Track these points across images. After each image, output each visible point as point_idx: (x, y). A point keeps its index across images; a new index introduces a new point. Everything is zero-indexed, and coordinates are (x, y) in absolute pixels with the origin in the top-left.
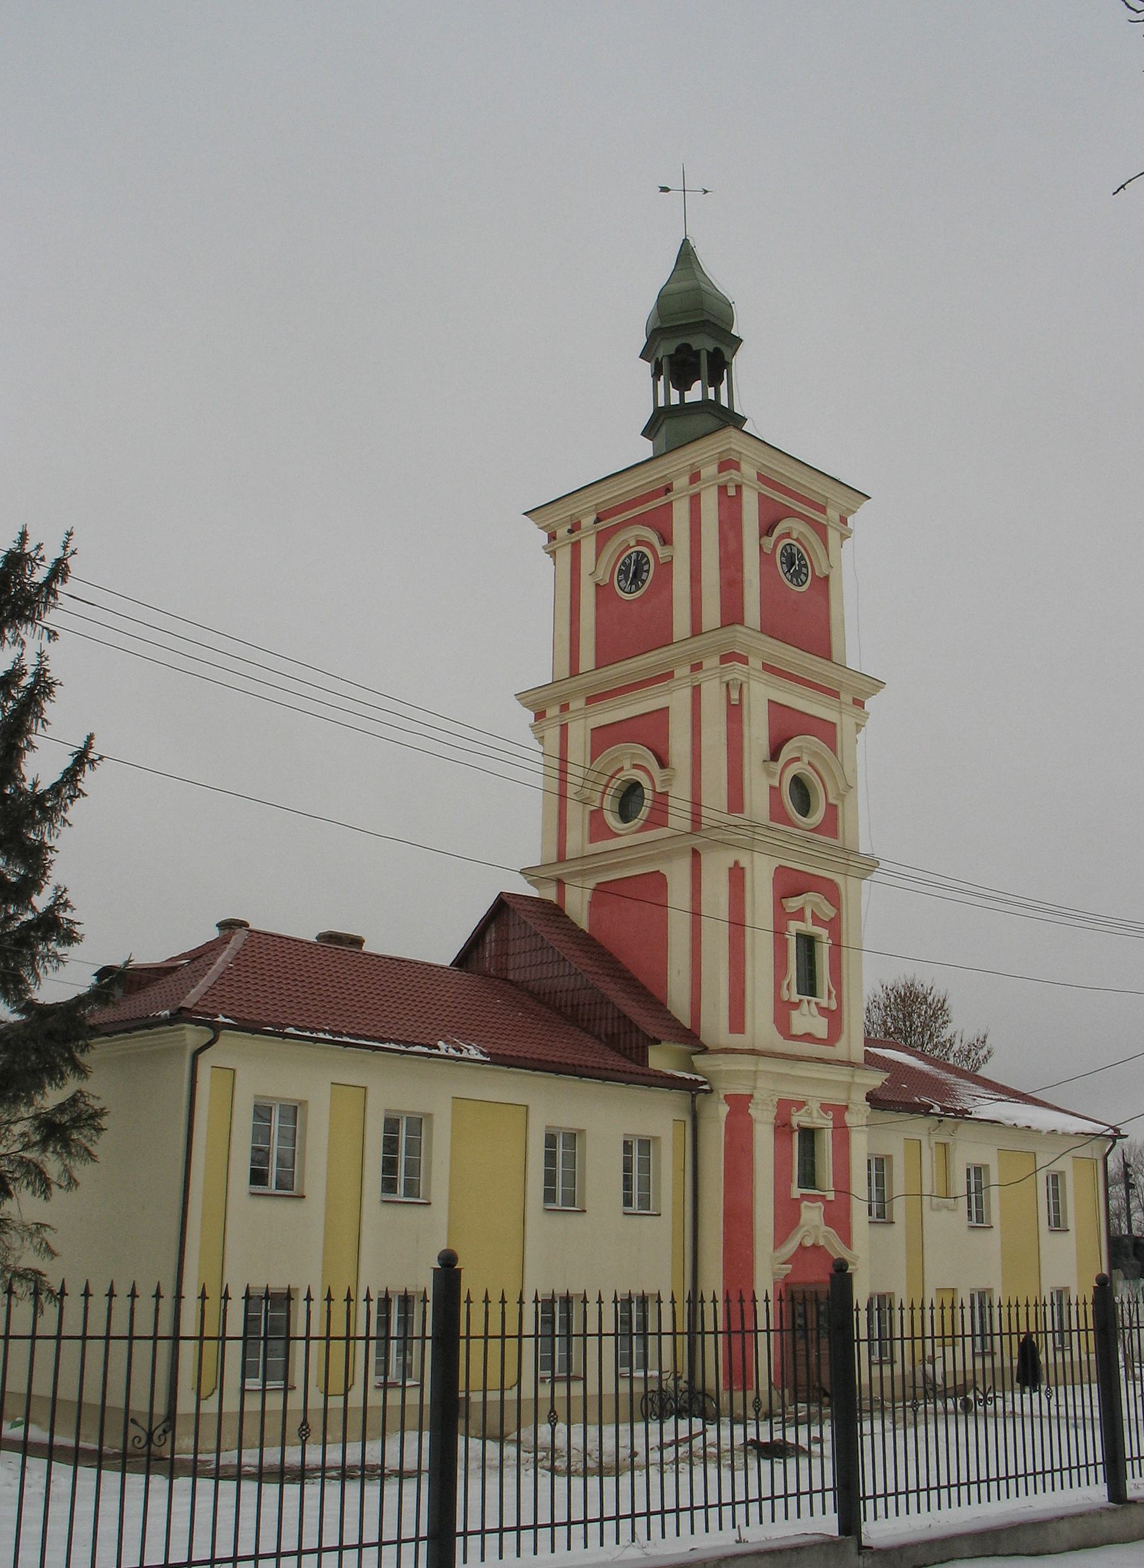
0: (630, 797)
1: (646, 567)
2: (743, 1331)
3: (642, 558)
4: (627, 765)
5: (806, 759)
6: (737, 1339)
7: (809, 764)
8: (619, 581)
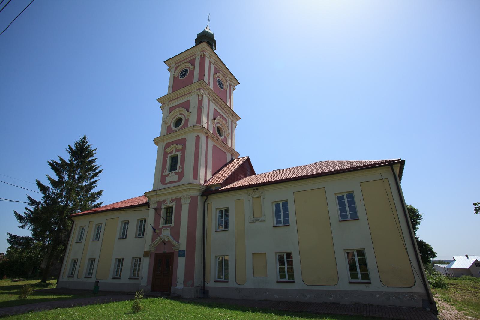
4: (178, 114)
5: (221, 124)
8: (180, 76)
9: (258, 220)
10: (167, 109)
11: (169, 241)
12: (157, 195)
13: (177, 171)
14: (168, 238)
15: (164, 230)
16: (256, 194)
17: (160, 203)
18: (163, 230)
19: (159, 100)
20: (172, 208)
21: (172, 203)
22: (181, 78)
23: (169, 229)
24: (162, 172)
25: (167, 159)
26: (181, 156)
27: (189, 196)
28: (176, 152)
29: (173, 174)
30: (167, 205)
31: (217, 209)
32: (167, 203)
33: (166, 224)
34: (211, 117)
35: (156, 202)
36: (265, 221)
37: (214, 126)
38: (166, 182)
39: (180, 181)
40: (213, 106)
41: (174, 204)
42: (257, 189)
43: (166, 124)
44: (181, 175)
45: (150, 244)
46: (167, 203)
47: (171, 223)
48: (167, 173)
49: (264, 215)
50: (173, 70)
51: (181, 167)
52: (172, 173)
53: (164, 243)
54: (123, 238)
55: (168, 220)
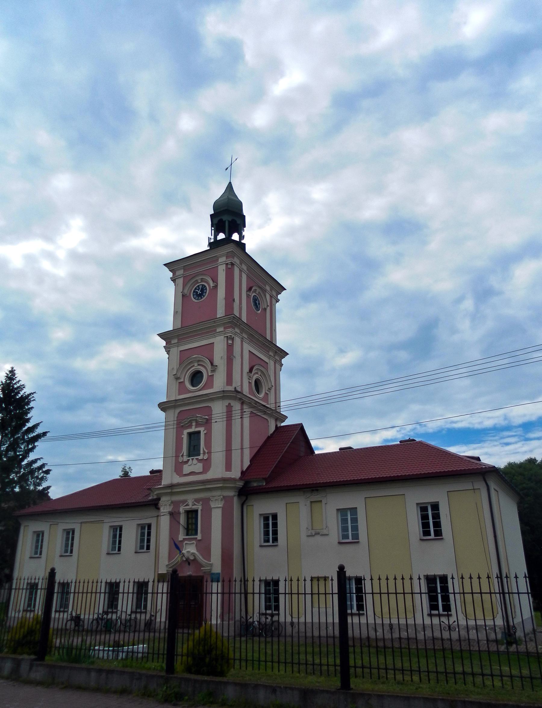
0: (196, 378)
1: (205, 291)
2: (230, 593)
3: (204, 287)
6: (226, 596)
7: (260, 375)
9: (318, 534)
10: (175, 351)
11: (195, 560)
12: (172, 494)
13: (200, 457)
14: (194, 556)
15: (186, 544)
16: (315, 497)
17: (176, 504)
18: (184, 544)
19: (161, 336)
20: (196, 511)
21: (195, 505)
22: (195, 299)
23: (194, 543)
24: (177, 457)
25: (183, 436)
26: (205, 434)
27: (222, 497)
28: (196, 427)
29: (195, 461)
30: (187, 508)
31: (261, 515)
32: (189, 505)
33: (187, 535)
34: (246, 369)
35: (170, 502)
36: (328, 535)
37: (251, 381)
38: (184, 473)
39: (206, 473)
40: (247, 347)
41: (199, 507)
42: (317, 490)
43: (177, 379)
44: (207, 464)
45: (167, 563)
46: (187, 505)
47: (196, 534)
48: (185, 459)
49: (326, 527)
50: (180, 281)
51: (206, 451)
52: (193, 459)
53: (188, 562)
54: (114, 552)
55: (191, 529)
